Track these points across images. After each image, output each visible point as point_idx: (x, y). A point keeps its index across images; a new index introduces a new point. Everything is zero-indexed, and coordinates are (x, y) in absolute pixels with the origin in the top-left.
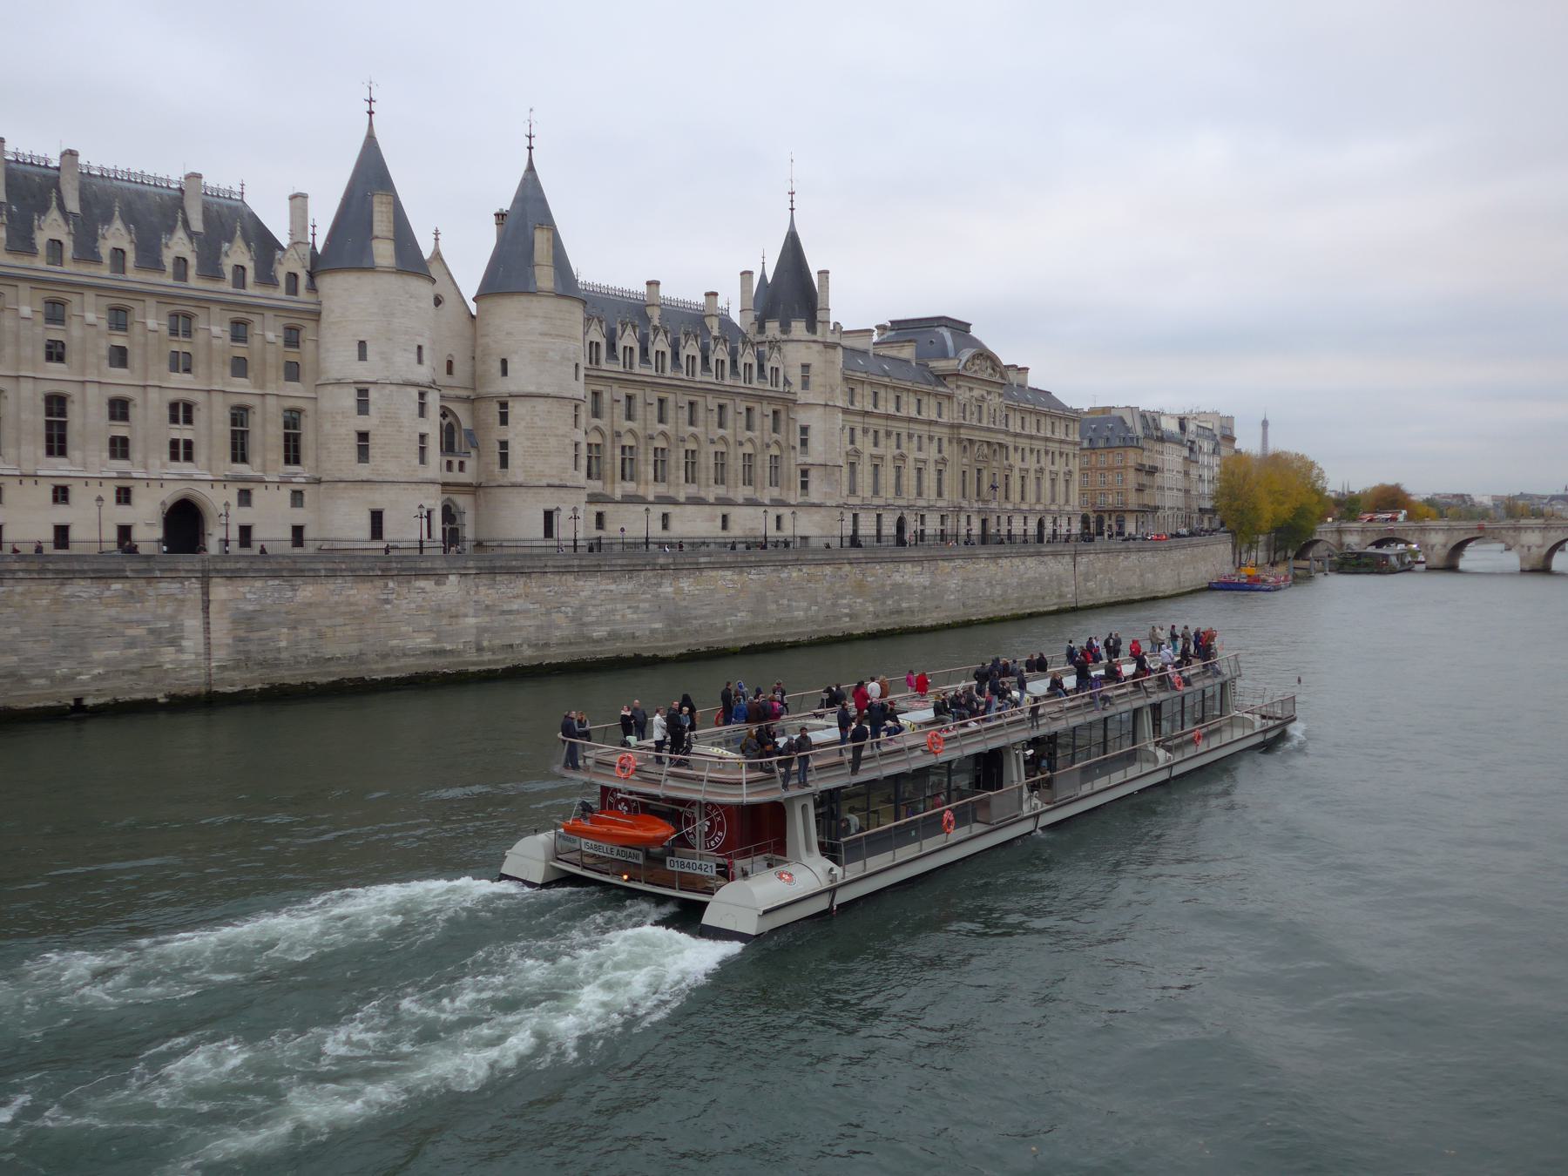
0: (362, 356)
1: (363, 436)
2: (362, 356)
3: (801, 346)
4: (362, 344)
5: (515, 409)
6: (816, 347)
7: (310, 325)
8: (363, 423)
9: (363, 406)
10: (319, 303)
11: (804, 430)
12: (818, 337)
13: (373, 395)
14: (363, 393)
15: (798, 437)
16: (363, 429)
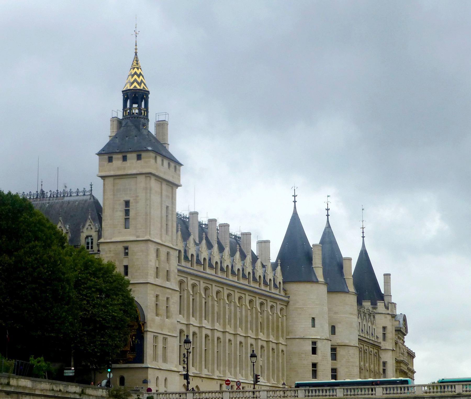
0: (314, 326)
1: (314, 365)
2: (314, 326)
3: (382, 316)
4: (313, 319)
5: (341, 352)
6: (389, 317)
7: (284, 307)
8: (314, 359)
9: (314, 351)
10: (289, 297)
11: (384, 363)
12: (389, 312)
13: (319, 345)
14: (314, 343)
15: (381, 368)
16: (315, 361)
